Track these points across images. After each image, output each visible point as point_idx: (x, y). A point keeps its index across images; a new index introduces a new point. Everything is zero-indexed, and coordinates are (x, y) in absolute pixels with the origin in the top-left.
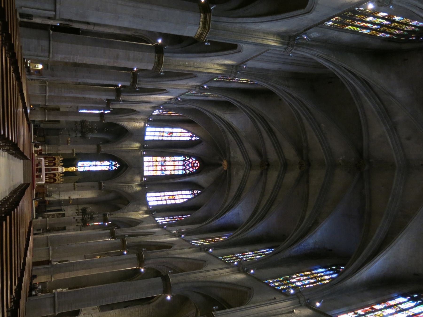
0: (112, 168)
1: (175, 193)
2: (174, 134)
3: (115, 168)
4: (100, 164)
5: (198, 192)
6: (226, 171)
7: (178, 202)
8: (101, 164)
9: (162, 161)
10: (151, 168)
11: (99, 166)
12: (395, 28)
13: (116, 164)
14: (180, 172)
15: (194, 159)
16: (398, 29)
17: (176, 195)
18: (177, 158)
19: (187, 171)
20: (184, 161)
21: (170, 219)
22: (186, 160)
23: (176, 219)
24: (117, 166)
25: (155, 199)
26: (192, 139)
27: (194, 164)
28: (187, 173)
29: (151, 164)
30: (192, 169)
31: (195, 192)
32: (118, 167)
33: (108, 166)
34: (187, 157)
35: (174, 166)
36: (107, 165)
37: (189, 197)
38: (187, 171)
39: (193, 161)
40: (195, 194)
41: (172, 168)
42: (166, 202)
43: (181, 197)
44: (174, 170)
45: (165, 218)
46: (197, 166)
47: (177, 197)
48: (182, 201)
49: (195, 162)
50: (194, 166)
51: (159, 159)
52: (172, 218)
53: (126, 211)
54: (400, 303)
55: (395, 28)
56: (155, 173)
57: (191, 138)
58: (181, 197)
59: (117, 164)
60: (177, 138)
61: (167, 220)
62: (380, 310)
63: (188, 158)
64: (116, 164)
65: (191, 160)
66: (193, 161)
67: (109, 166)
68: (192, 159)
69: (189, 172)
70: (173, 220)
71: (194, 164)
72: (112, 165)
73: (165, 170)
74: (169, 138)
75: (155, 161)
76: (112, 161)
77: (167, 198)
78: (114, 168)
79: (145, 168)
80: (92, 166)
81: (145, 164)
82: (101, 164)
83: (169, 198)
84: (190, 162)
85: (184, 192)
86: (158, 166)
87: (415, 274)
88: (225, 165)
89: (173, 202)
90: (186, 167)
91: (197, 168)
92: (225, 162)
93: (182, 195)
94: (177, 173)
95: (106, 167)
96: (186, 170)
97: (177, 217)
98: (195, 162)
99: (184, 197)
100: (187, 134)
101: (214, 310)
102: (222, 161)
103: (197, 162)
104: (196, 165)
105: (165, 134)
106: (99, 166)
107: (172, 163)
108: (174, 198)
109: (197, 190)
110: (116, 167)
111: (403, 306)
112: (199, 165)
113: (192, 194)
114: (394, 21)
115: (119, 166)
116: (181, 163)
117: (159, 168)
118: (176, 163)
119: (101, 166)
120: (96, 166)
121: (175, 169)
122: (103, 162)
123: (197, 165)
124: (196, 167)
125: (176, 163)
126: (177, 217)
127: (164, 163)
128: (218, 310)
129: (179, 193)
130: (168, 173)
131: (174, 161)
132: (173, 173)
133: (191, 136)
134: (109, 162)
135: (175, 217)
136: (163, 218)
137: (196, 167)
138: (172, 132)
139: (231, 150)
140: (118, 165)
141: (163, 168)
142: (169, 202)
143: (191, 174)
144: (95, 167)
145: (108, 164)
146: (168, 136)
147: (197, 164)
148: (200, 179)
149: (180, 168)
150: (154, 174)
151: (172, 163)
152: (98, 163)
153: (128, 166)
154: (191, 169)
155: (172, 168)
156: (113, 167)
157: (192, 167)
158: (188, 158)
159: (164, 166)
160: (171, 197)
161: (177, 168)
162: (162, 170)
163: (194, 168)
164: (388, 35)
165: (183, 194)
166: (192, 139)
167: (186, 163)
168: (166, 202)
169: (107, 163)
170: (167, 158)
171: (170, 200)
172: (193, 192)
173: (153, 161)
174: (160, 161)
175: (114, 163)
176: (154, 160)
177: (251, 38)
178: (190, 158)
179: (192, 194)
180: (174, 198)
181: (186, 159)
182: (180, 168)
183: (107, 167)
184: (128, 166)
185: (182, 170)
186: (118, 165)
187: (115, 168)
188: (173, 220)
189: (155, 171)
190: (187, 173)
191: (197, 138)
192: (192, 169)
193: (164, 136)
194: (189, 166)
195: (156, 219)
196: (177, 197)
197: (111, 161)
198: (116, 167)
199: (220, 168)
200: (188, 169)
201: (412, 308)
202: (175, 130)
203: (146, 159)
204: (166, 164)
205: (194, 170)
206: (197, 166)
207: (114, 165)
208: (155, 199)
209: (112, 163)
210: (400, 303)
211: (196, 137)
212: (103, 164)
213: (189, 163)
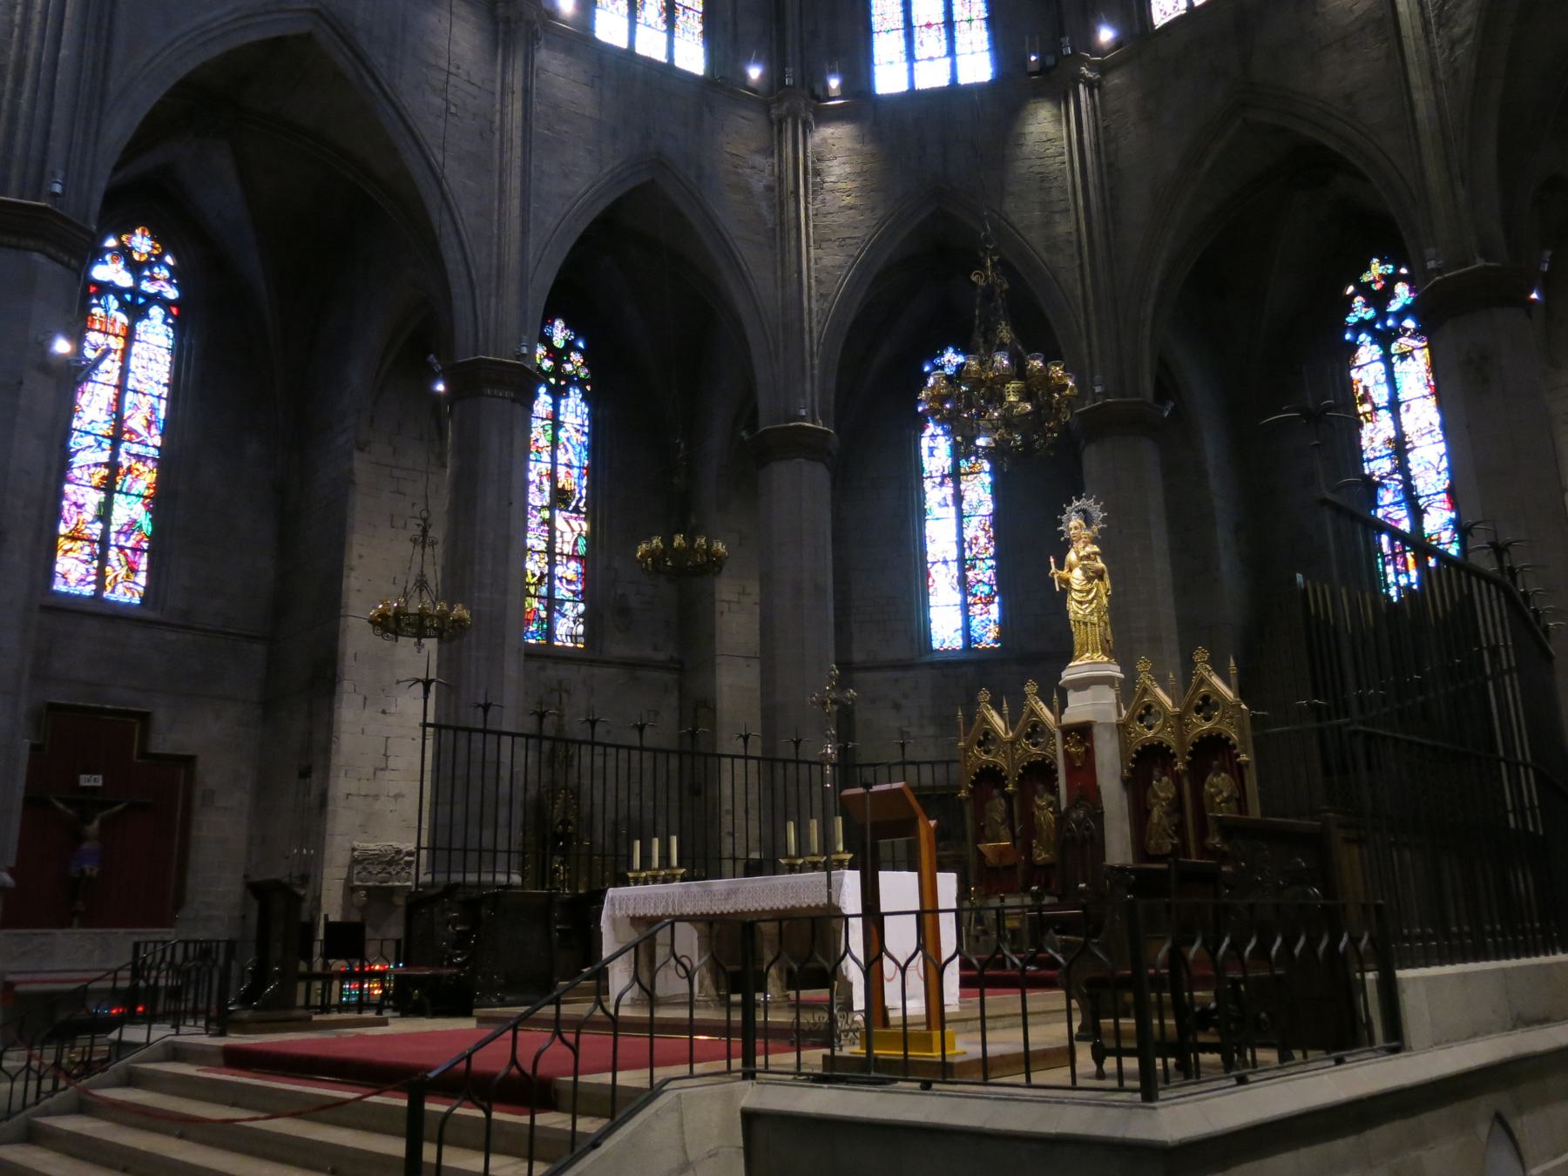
4: (1385, 417)
13: (1364, 289)
24: (1381, 276)
33: (1394, 348)
36: (1386, 358)
59: (1366, 278)
64: (1364, 289)
67: (1385, 339)
72: (1382, 315)
76: (1344, 328)
82: (1376, 408)
95: (1399, 367)
110: (1390, 280)
115: (1382, 263)
119: (1394, 405)
120: (1399, 447)
122: (1366, 398)
134: (1354, 347)
144: (1414, 459)
145: (1376, 351)
152: (1375, 435)
156: (1395, 306)
169: (1367, 370)
175: (1361, 311)
183: (1403, 357)
186: (1377, 269)
197: (1348, 336)
198: (1390, 280)
207: (1379, 299)
209: (1363, 325)
212: (1381, 395)
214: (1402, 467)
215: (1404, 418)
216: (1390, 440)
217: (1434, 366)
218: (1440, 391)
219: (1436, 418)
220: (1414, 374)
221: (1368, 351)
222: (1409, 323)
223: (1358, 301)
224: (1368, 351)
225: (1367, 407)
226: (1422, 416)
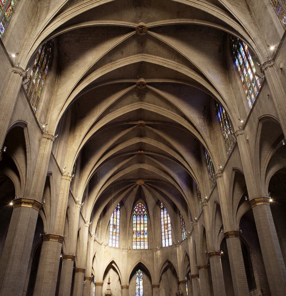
0: (142, 276)
1: (163, 223)
2: (115, 223)
3: (141, 273)
5: (162, 205)
6: (145, 182)
7: (169, 222)
8: (138, 285)
9: (136, 234)
10: (142, 243)
11: (139, 287)
12: (42, 63)
14: (146, 219)
15: (136, 207)
16: (43, 60)
17: (164, 223)
18: (134, 222)
19: (145, 213)
20: (137, 216)
21: (183, 228)
22: (136, 214)
23: (183, 223)
25: (167, 240)
26: (119, 209)
27: (139, 208)
28: (146, 213)
29: (138, 243)
30: (144, 209)
31: (162, 207)
32: (140, 271)
34: (134, 213)
35: (140, 224)
36: (139, 280)
37: (165, 212)
38: (145, 213)
39: (137, 208)
40: (163, 207)
41: (142, 226)
42: (170, 231)
43: (166, 219)
44: (144, 224)
45: (182, 232)
46: (141, 205)
47: (166, 222)
48: (169, 218)
49: (138, 206)
50: (141, 208)
51: (135, 236)
52: (182, 227)
53: (176, 265)
54: (239, 63)
55: (42, 63)
56: (146, 240)
57: (119, 210)
58: (166, 219)
59: (138, 271)
60: (118, 221)
61: (184, 231)
62: (244, 78)
63: (135, 212)
64: (138, 272)
65: (136, 210)
66: (137, 208)
67: (139, 278)
68: (135, 209)
69: (145, 212)
70: (184, 226)
71: (139, 208)
73: (144, 232)
74: (118, 227)
75: (136, 240)
77: (166, 231)
78: (141, 274)
79: (142, 247)
80: (139, 293)
81: (138, 247)
82: (138, 285)
83: (166, 229)
84: (138, 211)
85: (162, 216)
86: (140, 237)
87: (220, 52)
88: (140, 183)
89: (169, 225)
90: (142, 214)
91: (142, 205)
92: (140, 182)
93: (164, 218)
94: (146, 222)
95: (140, 281)
96: (144, 214)
97: (182, 222)
98: (138, 206)
99: (165, 216)
100: (115, 213)
101: (248, 200)
102: (137, 185)
103: (138, 205)
104: (140, 206)
105: (115, 231)
106: (139, 287)
107: (138, 226)
108: (166, 224)
109: (160, 206)
110: (140, 272)
111: (241, 62)
112: (140, 204)
113: (163, 210)
114: (37, 65)
116: (138, 219)
117: (142, 237)
118: (138, 222)
119: (139, 285)
120: (139, 289)
121: (143, 223)
122: (137, 283)
123: (140, 204)
124: (142, 206)
125: (138, 222)
126: (182, 222)
127: (138, 232)
128: (248, 197)
129: (162, 220)
130: (146, 229)
131: (137, 224)
132: (146, 225)
133: (117, 210)
135: (182, 224)
136: (183, 234)
137: (142, 206)
138: (113, 225)
139: (129, 178)
140: (139, 271)
141: (142, 233)
142: (170, 229)
143: (147, 210)
146: (116, 229)
147: (139, 205)
148: (151, 201)
149: (142, 219)
150: (147, 240)
151: (138, 226)
153: (140, 263)
154: (144, 210)
155: (142, 226)
156: (140, 275)
157: (142, 209)
158: (135, 212)
159: (140, 232)
160: (166, 227)
161: (142, 222)
162: (143, 234)
163: (142, 207)
164: (47, 67)
165: (163, 217)
166: (119, 209)
167: (139, 214)
168: (170, 231)
169: (137, 281)
170: (134, 229)
171: (168, 227)
172: (162, 208)
173: (136, 241)
174: (136, 236)
175: (137, 274)
176: (135, 241)
177: (42, 167)
178: (134, 211)
179: (163, 210)
180: (166, 224)
181: (135, 214)
182: (142, 219)
183: (141, 280)
184: (140, 263)
185: (144, 217)
186: (139, 271)
187: (141, 273)
188: (184, 226)
189: (144, 240)
190: (146, 213)
191: (119, 204)
192: (144, 209)
193: (116, 232)
194: (141, 211)
195: (183, 240)
196: (166, 222)
198: (140, 272)
199: (143, 186)
200: (144, 212)
201: (242, 57)
202: (111, 223)
203: (134, 247)
204: (139, 230)
205: (144, 207)
206: (141, 205)
208: (167, 240)
210: (239, 63)
211: (118, 206)
213: (138, 212)
214: (139, 292)
215: (140, 287)
216: (138, 289)
217: (143, 282)
218: (143, 285)
219: (143, 288)
220: (141, 282)
221: (138, 279)
222: (141, 277)
223: (137, 273)
224: (138, 279)
225: (137, 284)
226: (141, 287)
